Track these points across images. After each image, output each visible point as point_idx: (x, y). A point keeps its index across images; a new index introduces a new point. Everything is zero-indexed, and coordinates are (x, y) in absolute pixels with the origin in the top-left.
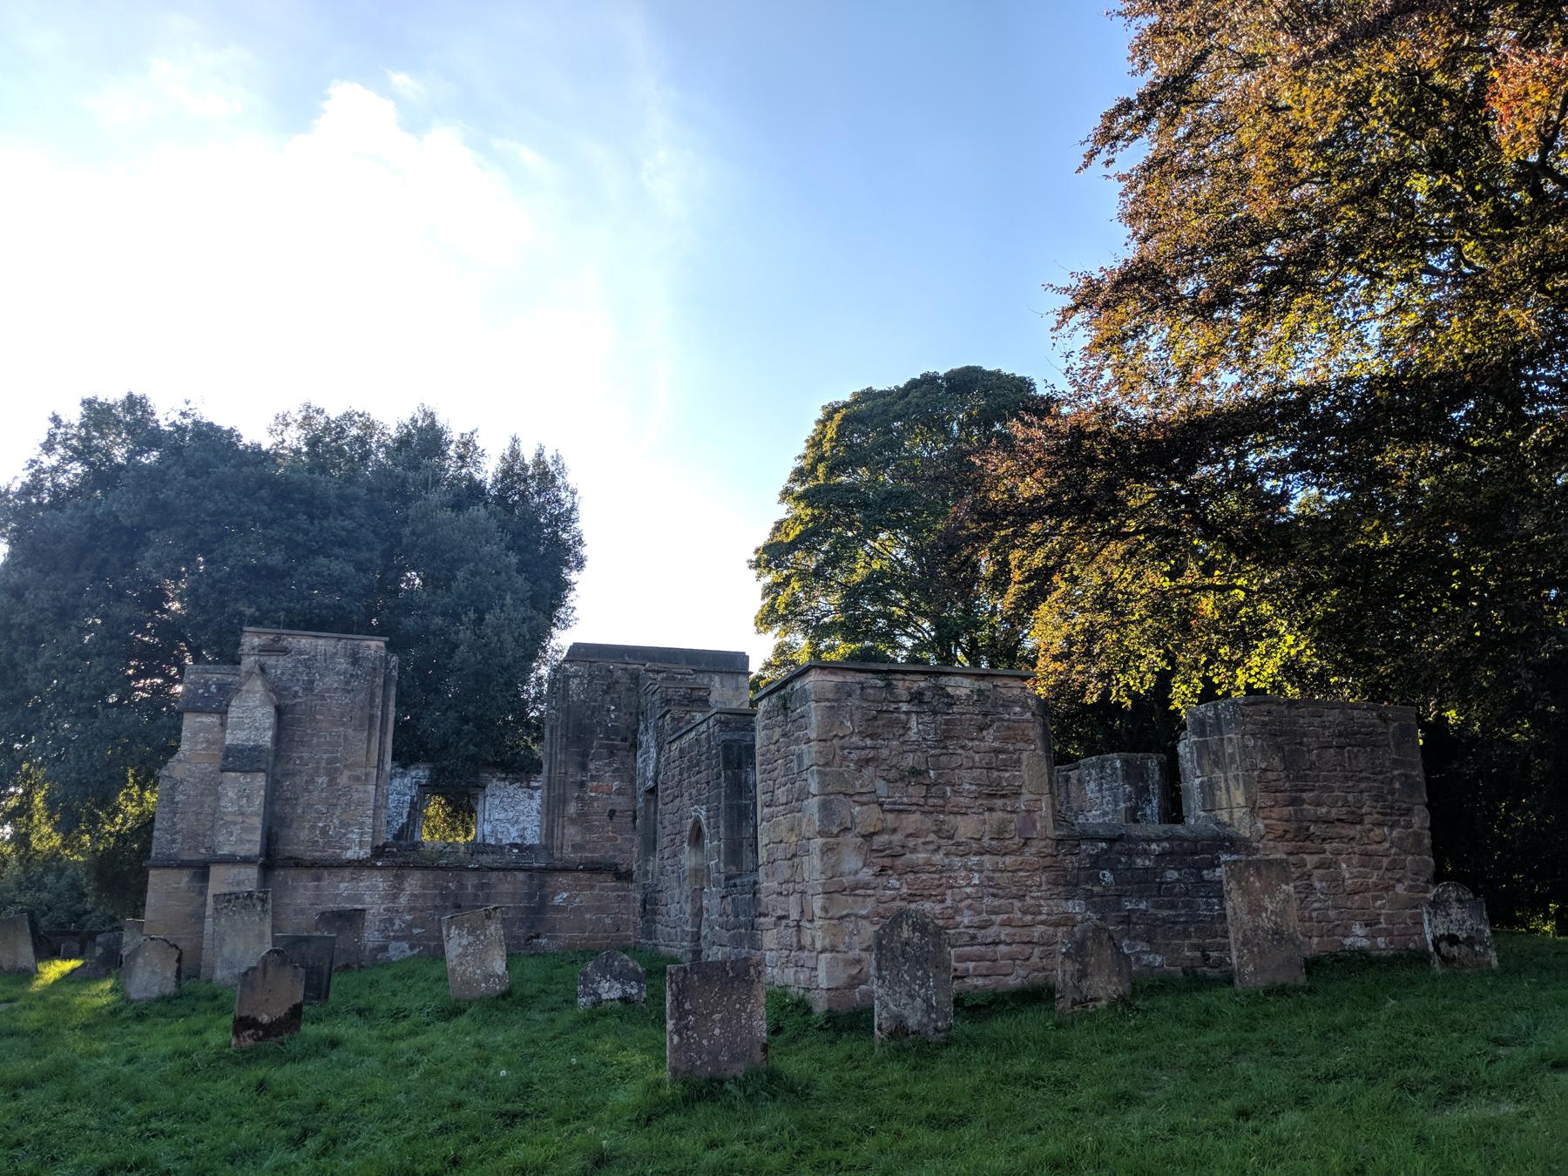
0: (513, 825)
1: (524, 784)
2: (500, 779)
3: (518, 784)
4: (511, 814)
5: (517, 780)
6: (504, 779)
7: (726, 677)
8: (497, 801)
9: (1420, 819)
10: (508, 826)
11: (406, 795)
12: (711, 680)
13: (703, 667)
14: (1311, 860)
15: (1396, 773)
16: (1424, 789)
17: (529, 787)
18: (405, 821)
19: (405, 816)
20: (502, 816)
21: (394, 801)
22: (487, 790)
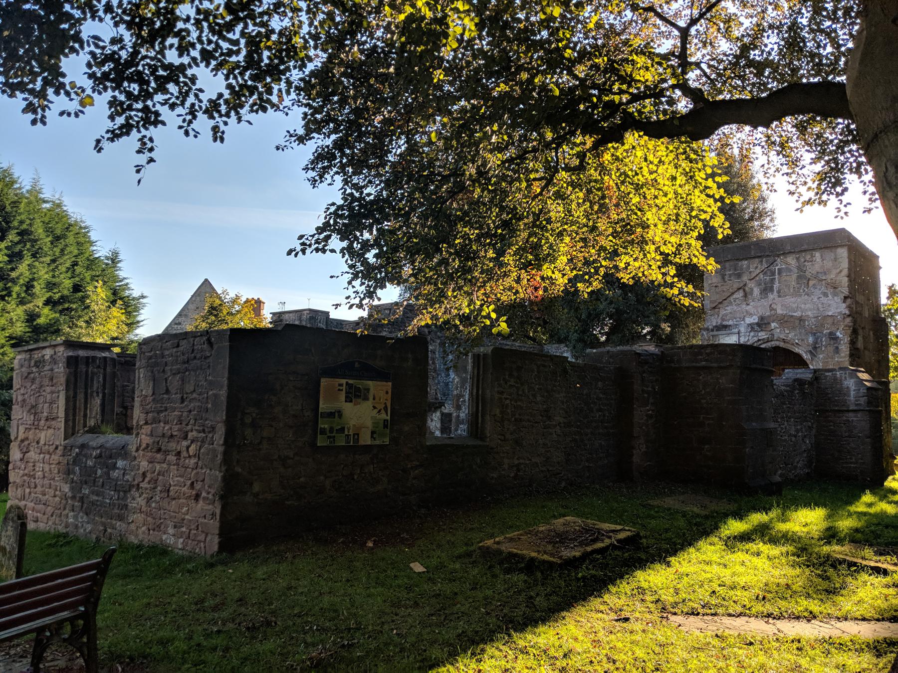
7: (826, 252)
9: (219, 436)
12: (812, 256)
13: (805, 247)
14: (158, 467)
15: (210, 393)
16: (224, 408)
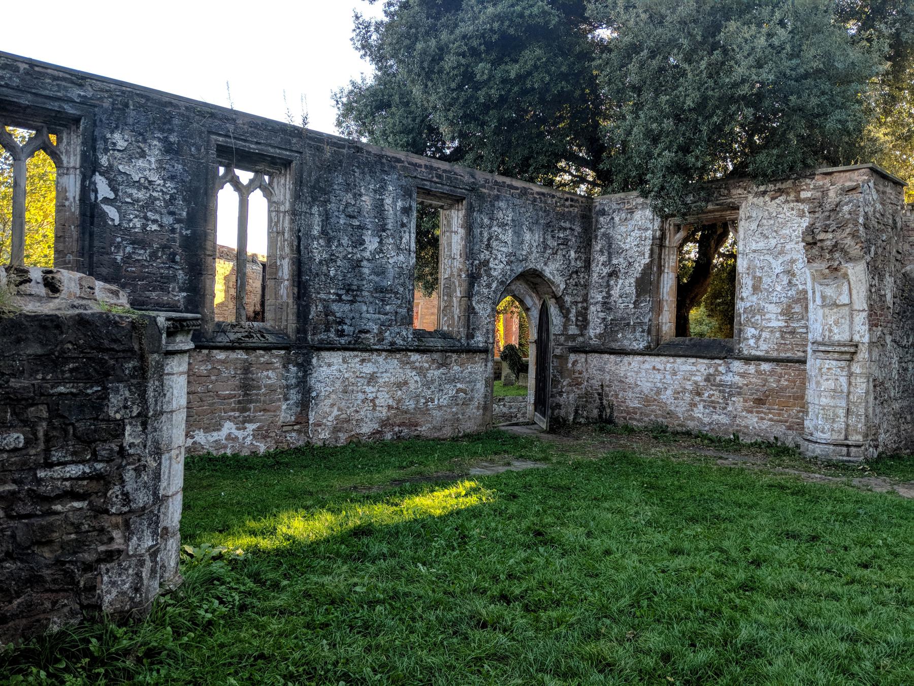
0: (776, 258)
1: (792, 196)
2: (757, 195)
3: (782, 198)
4: (773, 242)
5: (781, 191)
6: (764, 193)
8: (754, 226)
10: (770, 258)
11: (647, 229)
17: (798, 200)
18: (647, 260)
19: (647, 255)
20: (761, 245)
21: (636, 238)
22: (742, 213)
